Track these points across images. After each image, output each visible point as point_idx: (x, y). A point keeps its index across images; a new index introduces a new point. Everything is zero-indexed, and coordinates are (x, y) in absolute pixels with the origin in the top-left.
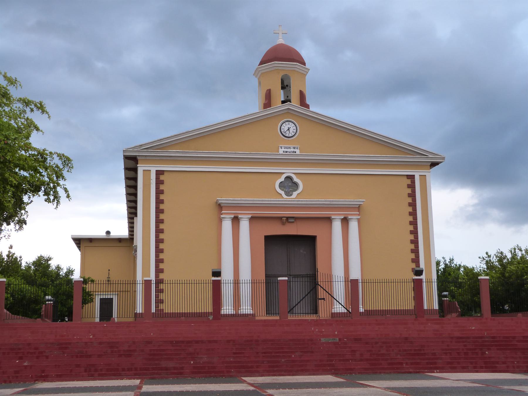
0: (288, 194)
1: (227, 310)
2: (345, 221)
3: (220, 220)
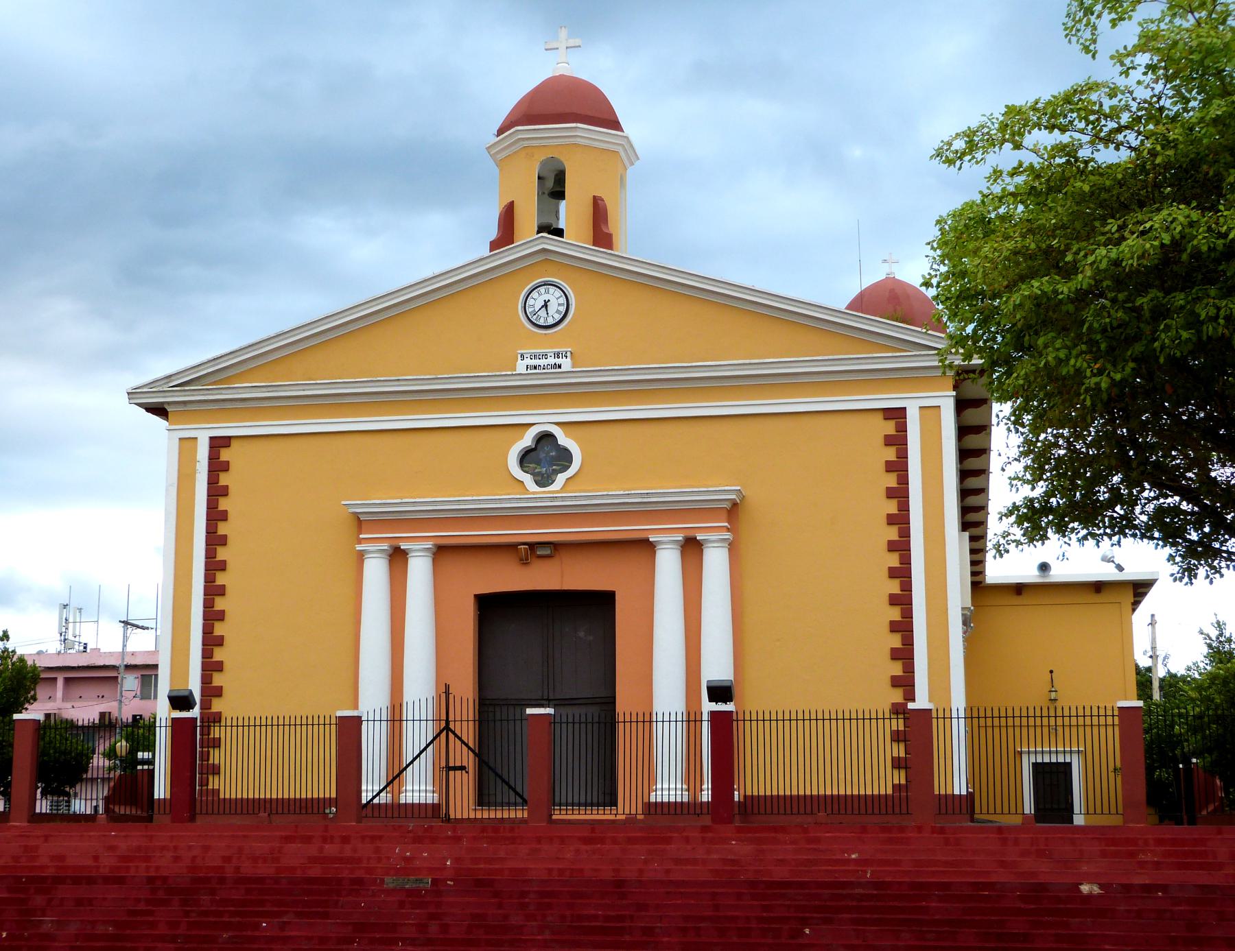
0: (543, 480)
1: (416, 794)
2: (692, 548)
3: (361, 556)
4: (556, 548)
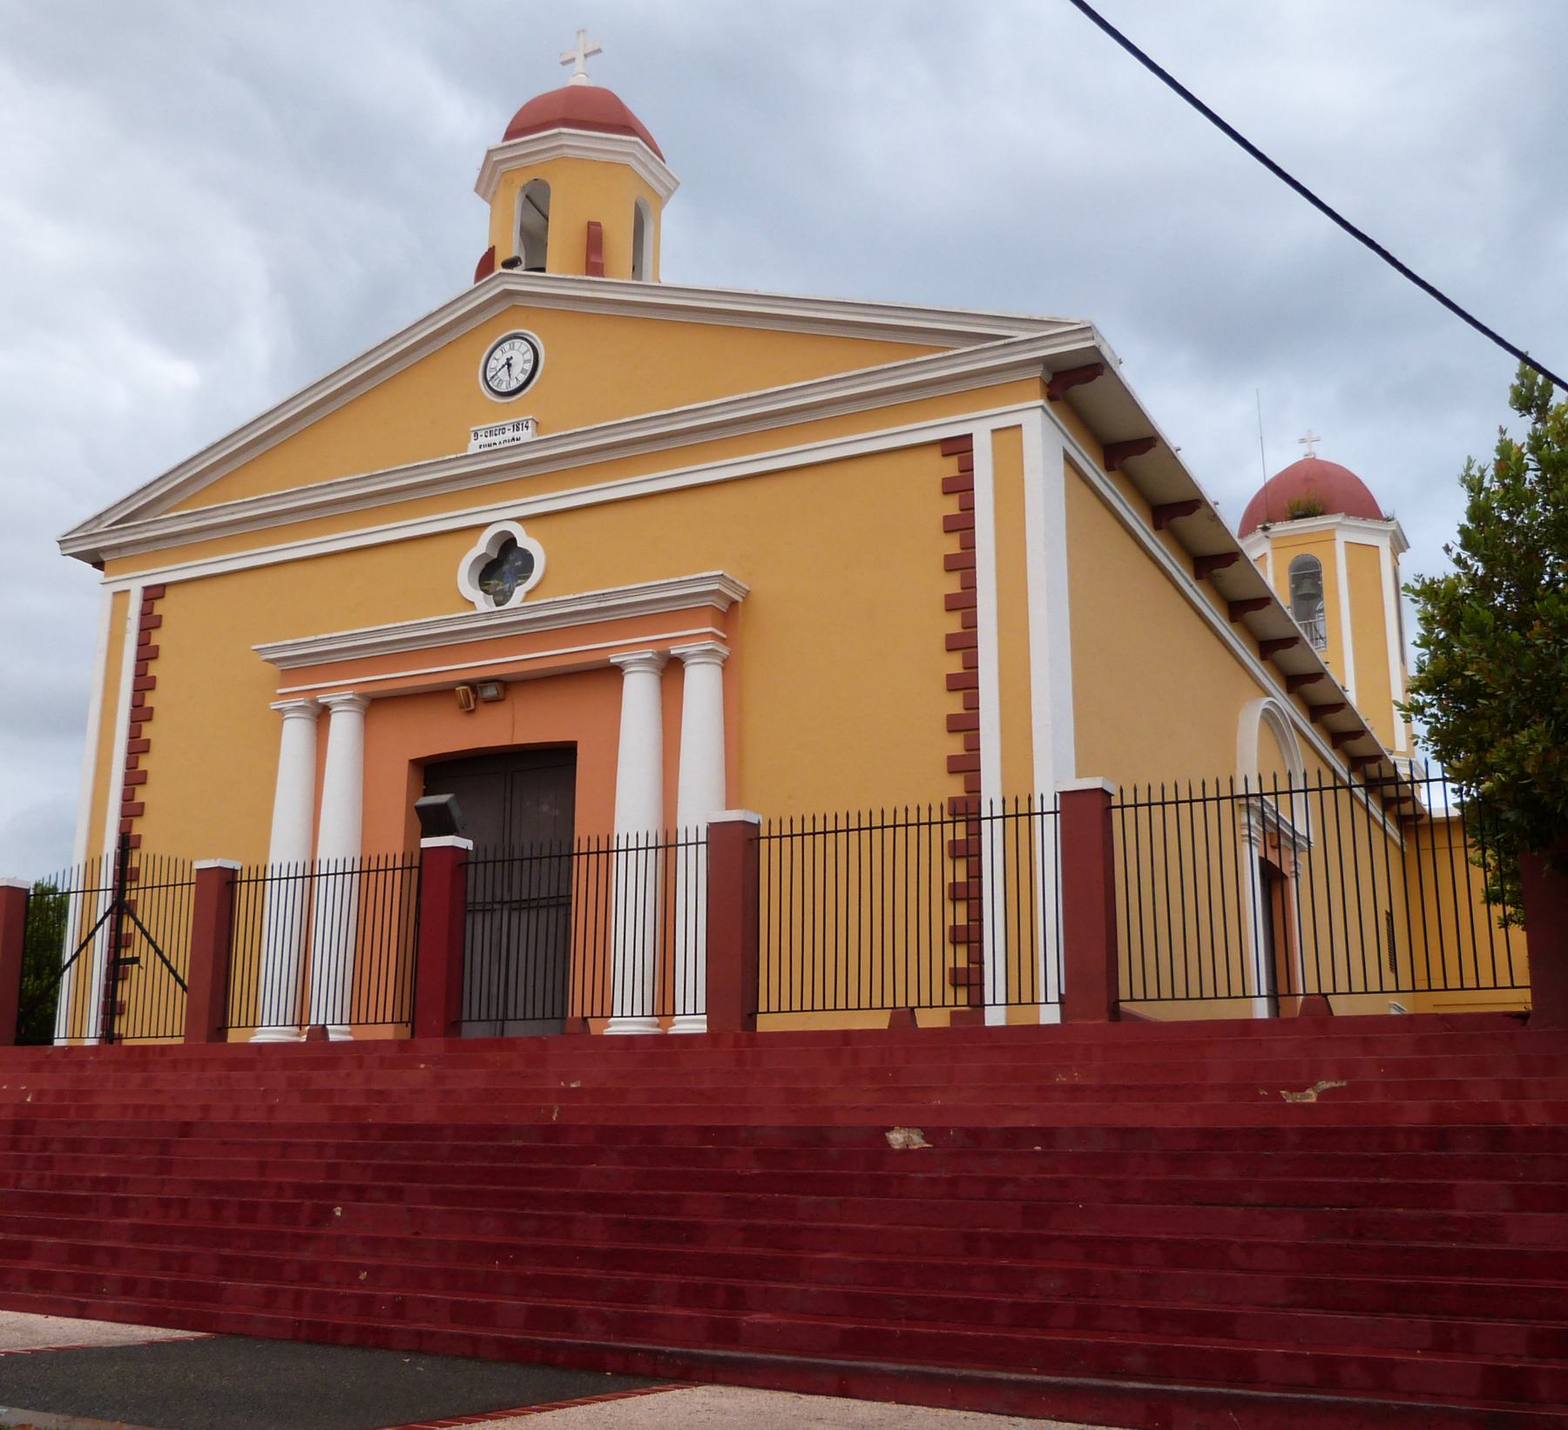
2: (671, 669)
4: (506, 687)
